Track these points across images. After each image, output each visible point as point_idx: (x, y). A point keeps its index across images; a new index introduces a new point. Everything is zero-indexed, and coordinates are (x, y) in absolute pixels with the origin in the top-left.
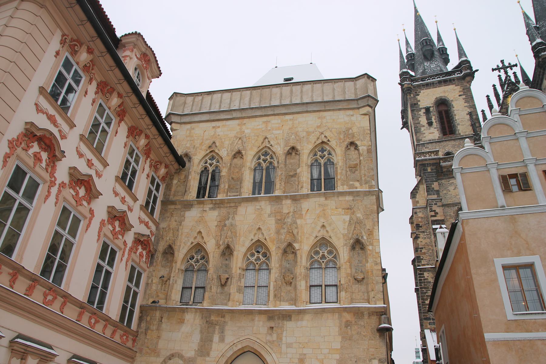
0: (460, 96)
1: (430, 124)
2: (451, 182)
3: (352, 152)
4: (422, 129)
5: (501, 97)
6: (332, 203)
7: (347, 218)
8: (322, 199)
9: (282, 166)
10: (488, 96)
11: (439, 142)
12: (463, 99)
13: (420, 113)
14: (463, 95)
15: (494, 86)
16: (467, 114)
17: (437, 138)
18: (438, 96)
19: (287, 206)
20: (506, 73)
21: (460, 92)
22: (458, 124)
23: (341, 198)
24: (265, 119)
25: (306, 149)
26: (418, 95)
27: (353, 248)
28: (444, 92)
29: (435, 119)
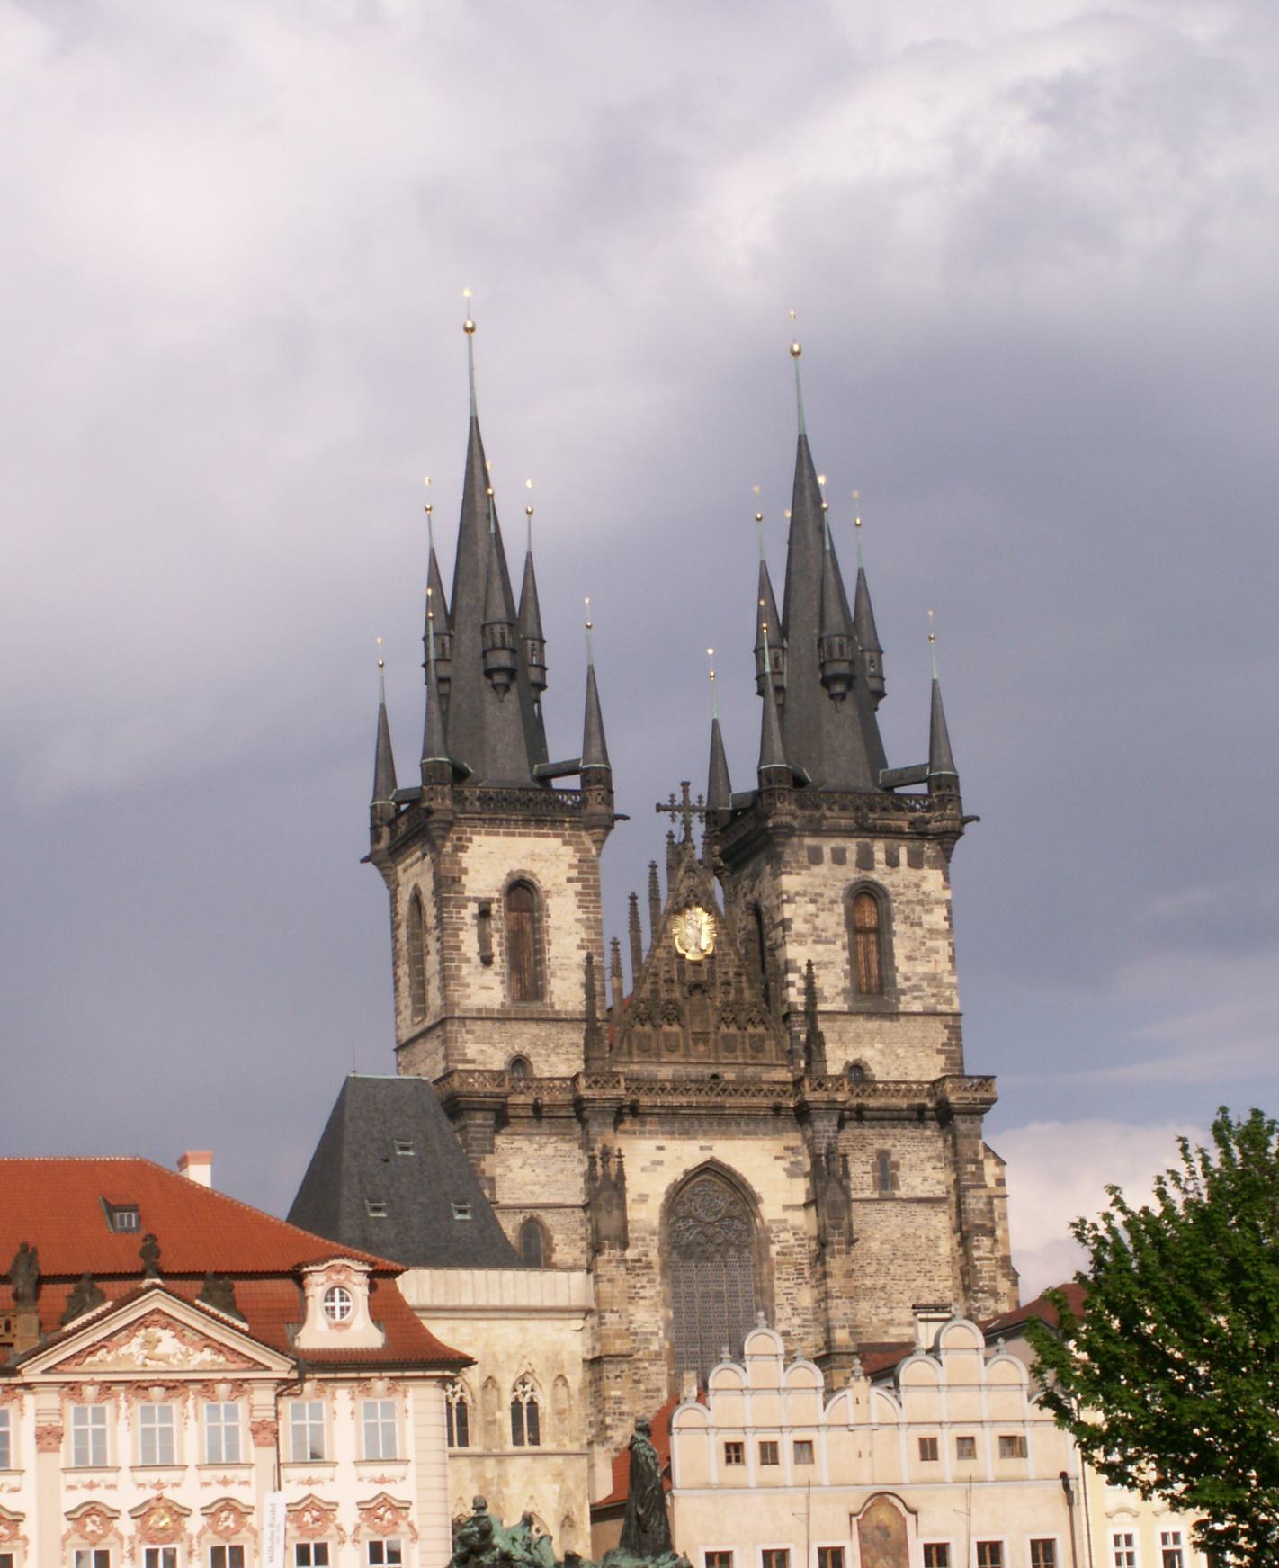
0: (569, 880)
1: (487, 961)
2: (517, 1144)
3: (562, 1392)
4: (465, 969)
5: (664, 903)
6: (539, 1466)
7: (557, 1487)
8: (528, 1460)
9: (479, 1407)
10: (633, 898)
11: (502, 1018)
12: (578, 894)
13: (464, 913)
14: (578, 880)
15: (653, 866)
16: (581, 947)
17: (497, 1006)
18: (516, 867)
19: (490, 1466)
20: (688, 829)
21: (571, 866)
22: (553, 975)
23: (551, 1460)
24: (451, 1323)
25: (507, 1381)
26: (464, 849)
27: (563, 1526)
28: (533, 856)
29: (500, 945)
